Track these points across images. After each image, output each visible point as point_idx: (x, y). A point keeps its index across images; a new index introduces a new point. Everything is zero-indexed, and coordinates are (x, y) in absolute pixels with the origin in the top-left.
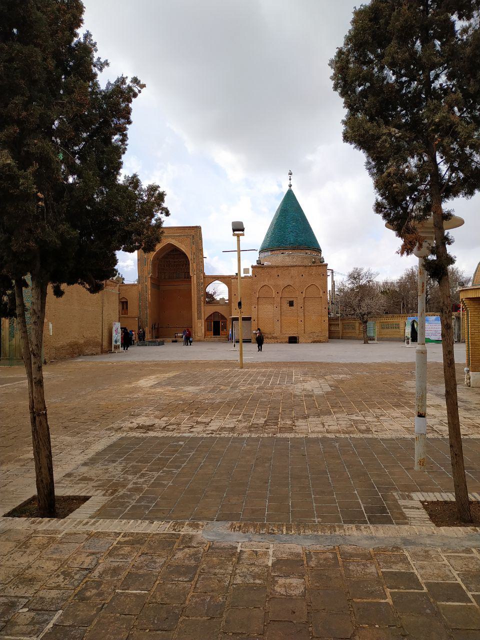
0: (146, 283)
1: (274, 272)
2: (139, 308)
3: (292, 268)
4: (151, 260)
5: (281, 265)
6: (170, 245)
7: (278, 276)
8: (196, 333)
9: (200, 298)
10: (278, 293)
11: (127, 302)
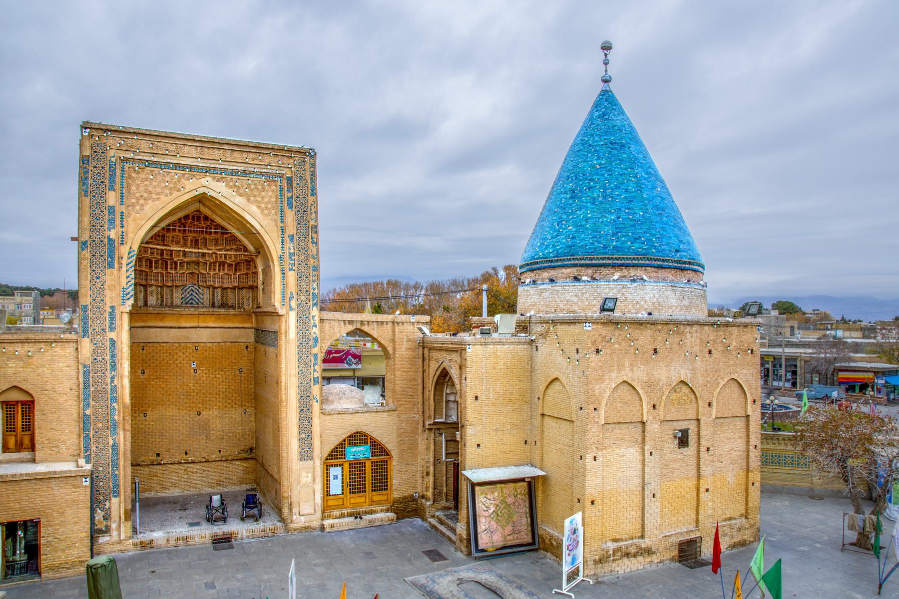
0: (113, 335)
1: (645, 337)
2: (86, 428)
3: (688, 329)
4: (136, 248)
6: (202, 199)
7: (655, 351)
8: (295, 505)
9: (309, 390)
10: (654, 406)
11: (29, 405)
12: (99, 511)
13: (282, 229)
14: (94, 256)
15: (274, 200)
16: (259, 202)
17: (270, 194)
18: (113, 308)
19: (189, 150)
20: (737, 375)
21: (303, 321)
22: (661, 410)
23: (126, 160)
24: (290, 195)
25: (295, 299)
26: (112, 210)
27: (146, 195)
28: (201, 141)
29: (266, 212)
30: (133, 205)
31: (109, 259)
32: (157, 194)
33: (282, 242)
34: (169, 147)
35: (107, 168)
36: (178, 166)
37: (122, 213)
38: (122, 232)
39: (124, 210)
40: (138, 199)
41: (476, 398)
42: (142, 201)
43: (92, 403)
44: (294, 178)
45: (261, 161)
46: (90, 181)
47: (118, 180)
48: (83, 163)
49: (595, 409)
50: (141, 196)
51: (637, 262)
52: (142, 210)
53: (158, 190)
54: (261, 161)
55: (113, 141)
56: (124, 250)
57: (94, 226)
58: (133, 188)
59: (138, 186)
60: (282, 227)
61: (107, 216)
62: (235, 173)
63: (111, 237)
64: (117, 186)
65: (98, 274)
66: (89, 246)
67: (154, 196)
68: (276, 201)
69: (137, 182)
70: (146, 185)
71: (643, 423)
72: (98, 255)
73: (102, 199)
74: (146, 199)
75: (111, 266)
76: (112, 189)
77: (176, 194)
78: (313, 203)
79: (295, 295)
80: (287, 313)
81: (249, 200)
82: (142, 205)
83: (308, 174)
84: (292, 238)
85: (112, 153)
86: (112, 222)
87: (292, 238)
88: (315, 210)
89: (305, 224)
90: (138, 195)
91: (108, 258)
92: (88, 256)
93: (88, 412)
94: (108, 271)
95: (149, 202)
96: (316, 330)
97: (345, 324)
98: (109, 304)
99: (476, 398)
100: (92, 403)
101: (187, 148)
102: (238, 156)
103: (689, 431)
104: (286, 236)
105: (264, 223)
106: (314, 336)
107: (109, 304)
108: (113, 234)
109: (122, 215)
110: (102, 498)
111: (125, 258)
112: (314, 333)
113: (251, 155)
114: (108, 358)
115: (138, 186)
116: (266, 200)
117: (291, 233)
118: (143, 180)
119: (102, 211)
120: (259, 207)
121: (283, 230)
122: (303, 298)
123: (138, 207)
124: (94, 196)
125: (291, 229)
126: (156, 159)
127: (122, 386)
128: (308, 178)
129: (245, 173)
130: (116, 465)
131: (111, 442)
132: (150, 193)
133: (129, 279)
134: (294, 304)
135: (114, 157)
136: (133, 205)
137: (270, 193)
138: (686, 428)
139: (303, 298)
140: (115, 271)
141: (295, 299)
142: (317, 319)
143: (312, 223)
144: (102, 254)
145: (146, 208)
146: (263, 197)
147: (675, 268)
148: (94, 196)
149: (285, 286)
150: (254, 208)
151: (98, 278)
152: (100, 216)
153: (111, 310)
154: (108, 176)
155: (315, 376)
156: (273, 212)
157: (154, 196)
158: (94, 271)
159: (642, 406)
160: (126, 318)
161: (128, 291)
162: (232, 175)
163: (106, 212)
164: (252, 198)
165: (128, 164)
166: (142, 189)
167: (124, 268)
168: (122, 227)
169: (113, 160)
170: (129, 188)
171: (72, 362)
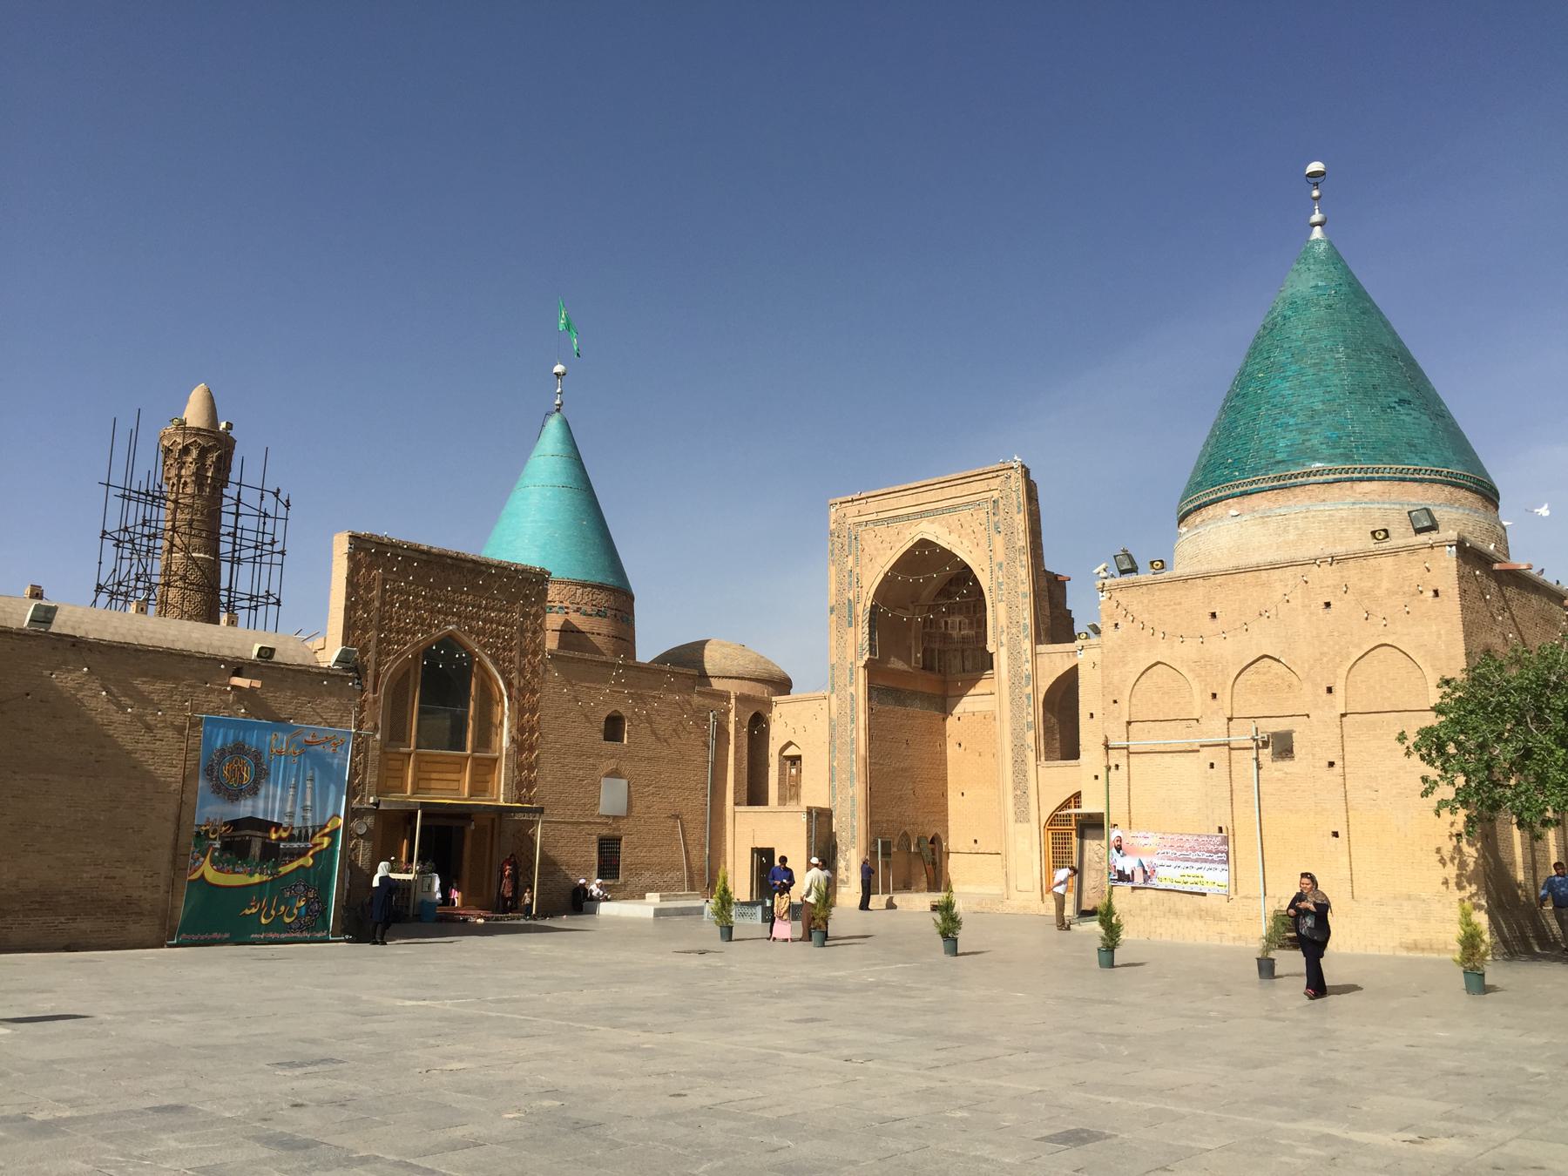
0: (852, 689)
2: (831, 780)
5: (1229, 564)
6: (924, 544)
7: (1214, 615)
10: (1214, 696)
12: (842, 861)
18: (851, 663)
20: (1394, 637)
21: (1014, 656)
22: (1225, 697)
24: (996, 519)
25: (1005, 634)
41: (1092, 715)
43: (838, 755)
49: (1115, 702)
51: (1214, 496)
56: (860, 608)
67: (882, 552)
79: (1005, 629)
84: (1000, 565)
87: (1000, 565)
93: (835, 764)
96: (1028, 666)
97: (1069, 656)
98: (850, 661)
99: (1092, 715)
100: (838, 755)
103: (1294, 735)
110: (844, 848)
111: (861, 615)
114: (848, 711)
117: (999, 560)
122: (1014, 631)
123: (870, 566)
125: (1000, 555)
127: (858, 738)
130: (853, 816)
131: (851, 793)
133: (864, 635)
134: (1004, 638)
138: (1286, 729)
139: (1014, 631)
141: (1005, 634)
142: (1029, 652)
147: (1273, 489)
149: (996, 619)
155: (1029, 720)
157: (882, 552)
159: (1192, 695)
167: (860, 627)
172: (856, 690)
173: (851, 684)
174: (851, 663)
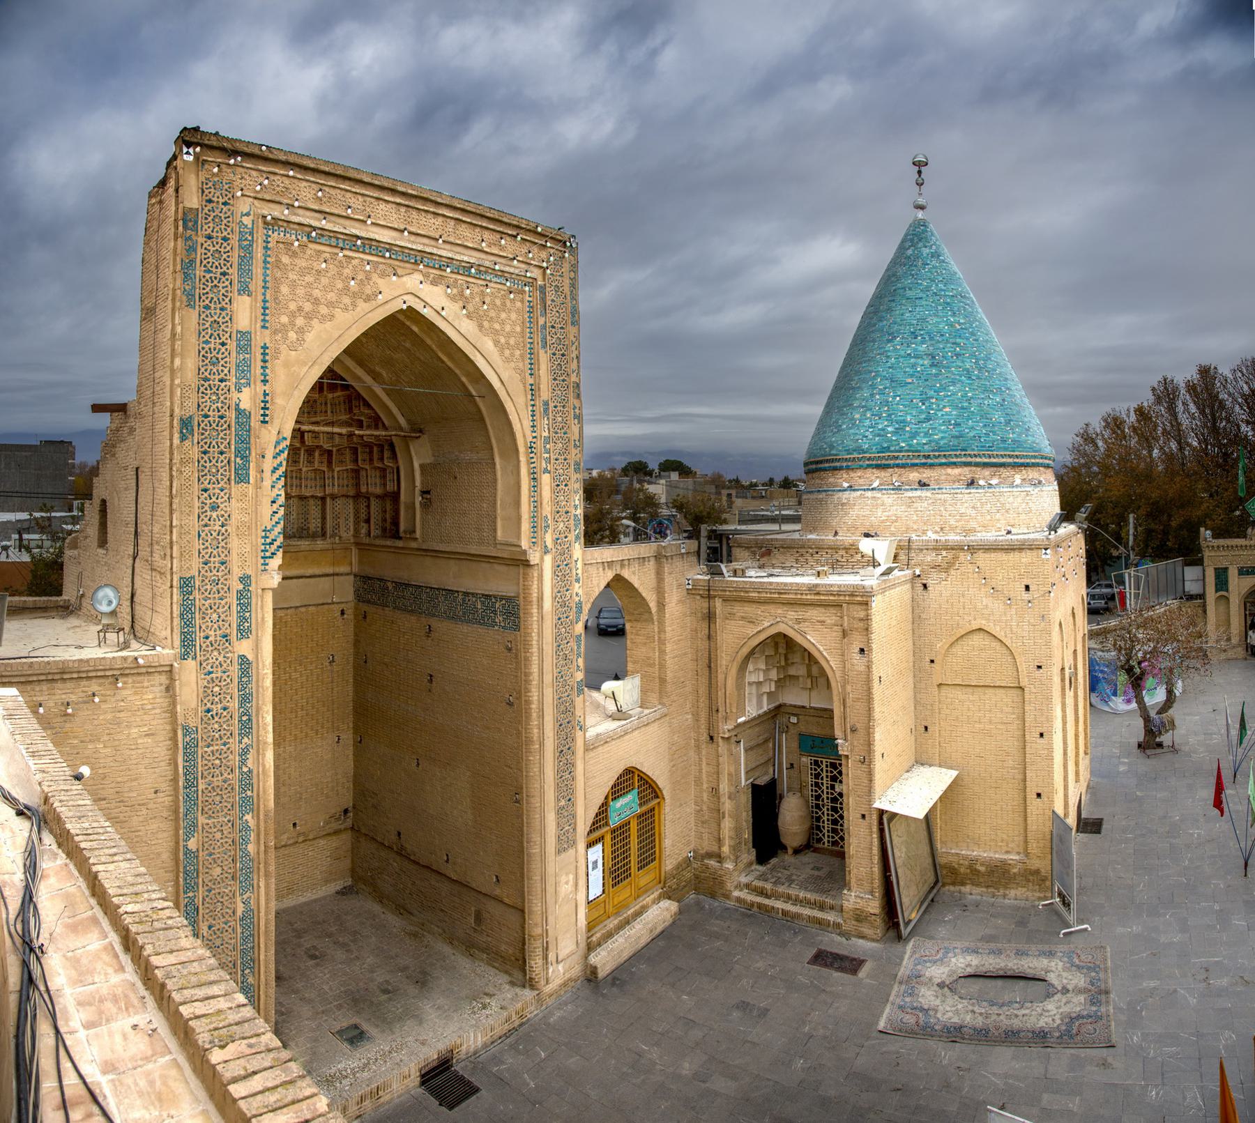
0: (244, 647)
4: (288, 433)
13: (532, 390)
14: (205, 453)
15: (518, 329)
16: (496, 332)
17: (512, 318)
18: (245, 579)
19: (386, 212)
23: (273, 224)
26: (244, 340)
27: (308, 307)
28: (404, 194)
29: (507, 352)
30: (283, 330)
31: (238, 460)
32: (330, 305)
33: (533, 416)
34: (356, 202)
35: (234, 240)
36: (371, 245)
37: (265, 347)
38: (265, 394)
39: (267, 341)
40: (293, 315)
42: (300, 321)
44: (548, 289)
45: (502, 248)
46: (199, 272)
47: (258, 270)
48: (185, 227)
50: (300, 309)
52: (300, 341)
53: (331, 296)
54: (502, 248)
55: (249, 179)
57: (206, 379)
58: (285, 289)
59: (293, 286)
60: (532, 385)
61: (234, 354)
62: (465, 269)
63: (242, 406)
64: (256, 284)
65: (214, 499)
66: (196, 428)
67: (324, 310)
68: (523, 331)
69: (292, 276)
70: (309, 285)
71: (1022, 689)
72: (214, 451)
73: (224, 313)
74: (309, 317)
75: (242, 477)
76: (245, 290)
77: (362, 306)
78: (574, 340)
80: (542, 559)
81: (481, 326)
82: (301, 331)
83: (567, 281)
85: (244, 206)
86: (244, 369)
88: (577, 352)
89: (564, 380)
90: (293, 306)
91: (236, 456)
92: (195, 453)
94: (236, 490)
95: (315, 322)
98: (237, 572)
101: (382, 206)
102: (469, 236)
104: (540, 404)
105: (505, 377)
106: (577, 599)
107: (237, 572)
108: (246, 399)
109: (264, 354)
112: (577, 594)
113: (486, 235)
115: (293, 286)
116: (508, 328)
118: (303, 272)
119: (223, 344)
120: (496, 343)
121: (534, 390)
123: (292, 335)
124: (207, 307)
126: (329, 226)
128: (567, 290)
129: (482, 270)
132: (316, 302)
134: (549, 539)
135: (248, 214)
136: (283, 330)
137: (514, 316)
140: (250, 490)
143: (574, 378)
144: (222, 447)
145: (309, 337)
146: (503, 323)
148: (207, 307)
149: (537, 504)
150: (488, 345)
151: (214, 508)
152: (220, 356)
153: (241, 587)
154: (235, 260)
156: (518, 353)
158: (205, 490)
160: (269, 598)
161: (272, 536)
162: (458, 273)
163: (232, 345)
164: (486, 324)
165: (276, 233)
166: (300, 291)
167: (267, 483)
168: (265, 381)
169: (247, 221)
170: (277, 290)
171: (159, 723)
172: (257, 648)
173: (244, 633)
174: (245, 579)
